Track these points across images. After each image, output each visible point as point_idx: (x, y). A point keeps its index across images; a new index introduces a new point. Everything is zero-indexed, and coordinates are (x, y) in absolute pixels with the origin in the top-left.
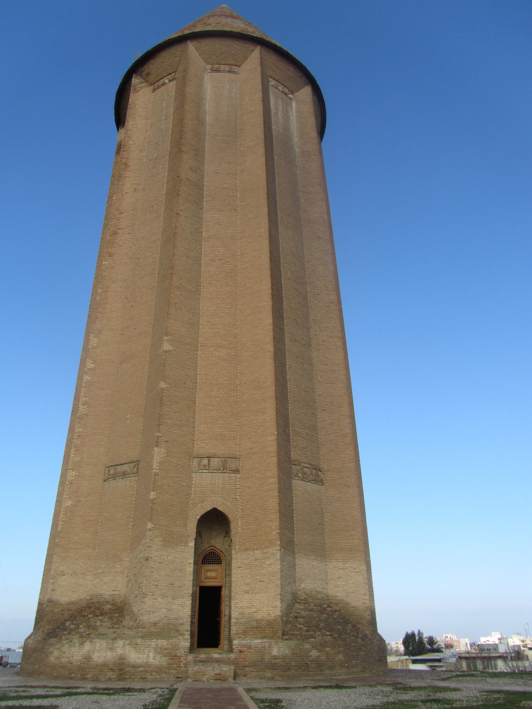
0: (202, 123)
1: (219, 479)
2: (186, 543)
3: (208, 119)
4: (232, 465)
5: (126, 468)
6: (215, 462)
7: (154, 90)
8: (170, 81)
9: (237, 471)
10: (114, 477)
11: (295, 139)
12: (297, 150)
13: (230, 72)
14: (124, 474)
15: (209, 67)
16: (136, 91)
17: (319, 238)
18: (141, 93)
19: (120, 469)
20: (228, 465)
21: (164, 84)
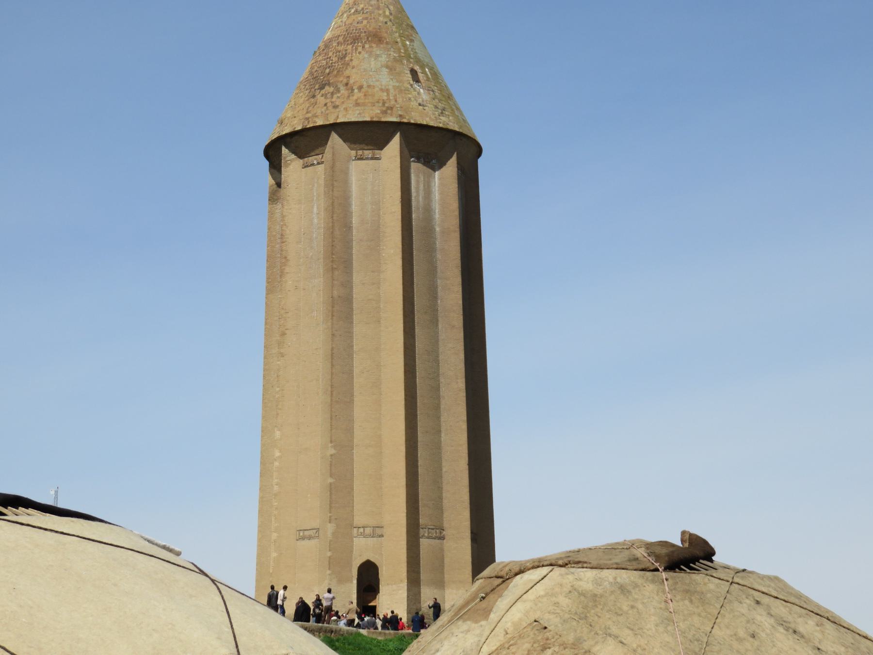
0: (348, 227)
1: (371, 541)
2: (352, 582)
3: (355, 221)
4: (378, 531)
5: (311, 533)
6: (368, 531)
7: (305, 166)
8: (318, 164)
9: (382, 536)
10: (303, 538)
11: (437, 216)
12: (438, 229)
13: (372, 159)
14: (310, 538)
15: (353, 153)
16: (287, 166)
17: (453, 326)
18: (291, 167)
19: (307, 533)
20: (377, 532)
21: (313, 165)
